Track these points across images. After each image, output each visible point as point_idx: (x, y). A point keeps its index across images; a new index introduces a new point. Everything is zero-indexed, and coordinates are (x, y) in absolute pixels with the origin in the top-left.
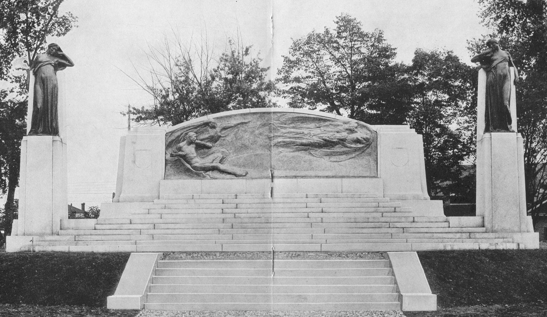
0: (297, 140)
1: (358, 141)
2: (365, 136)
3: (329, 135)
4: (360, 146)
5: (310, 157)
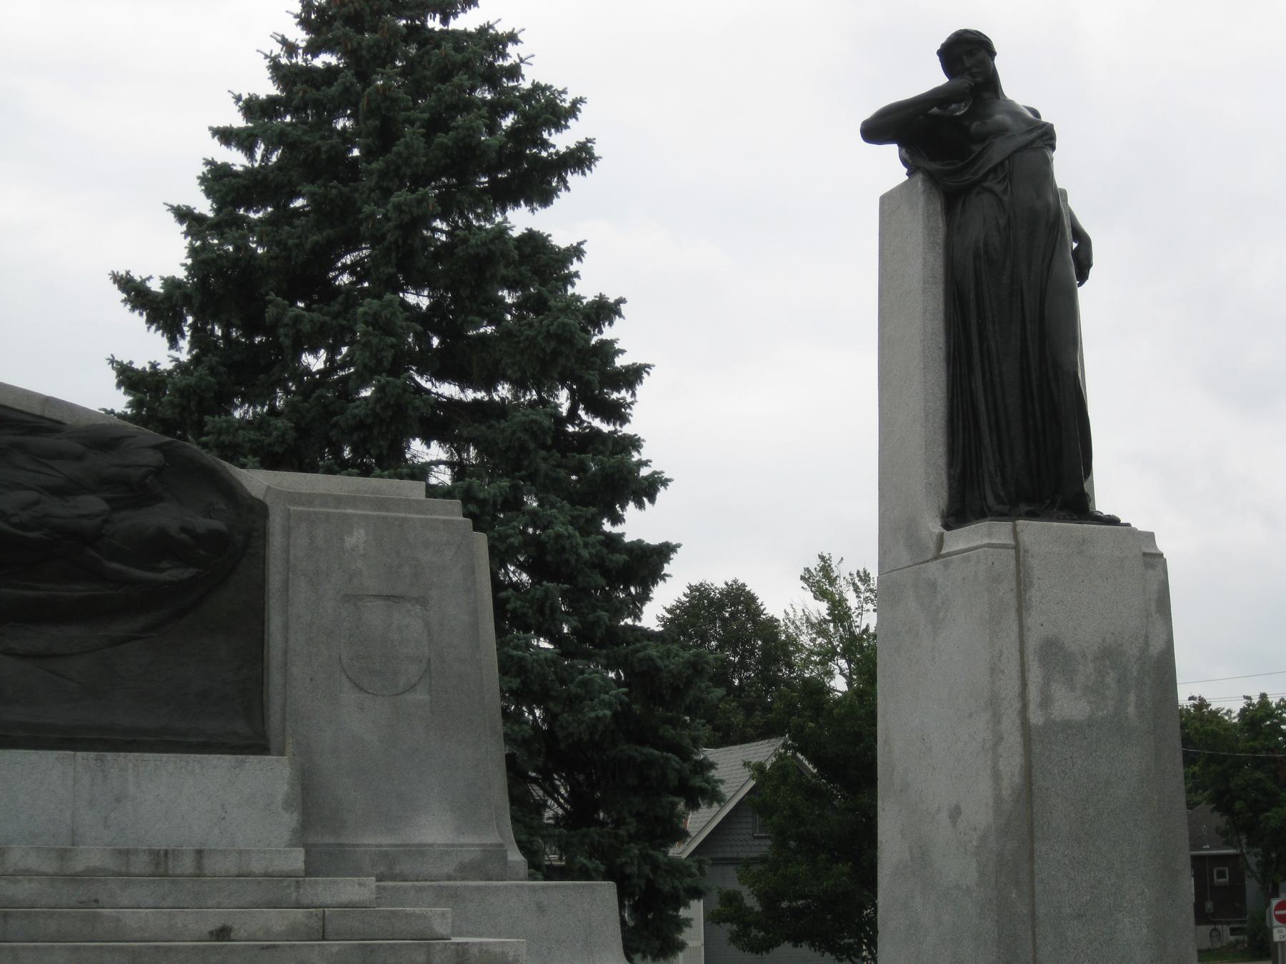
1: (161, 547)
2: (203, 524)
4: (172, 573)
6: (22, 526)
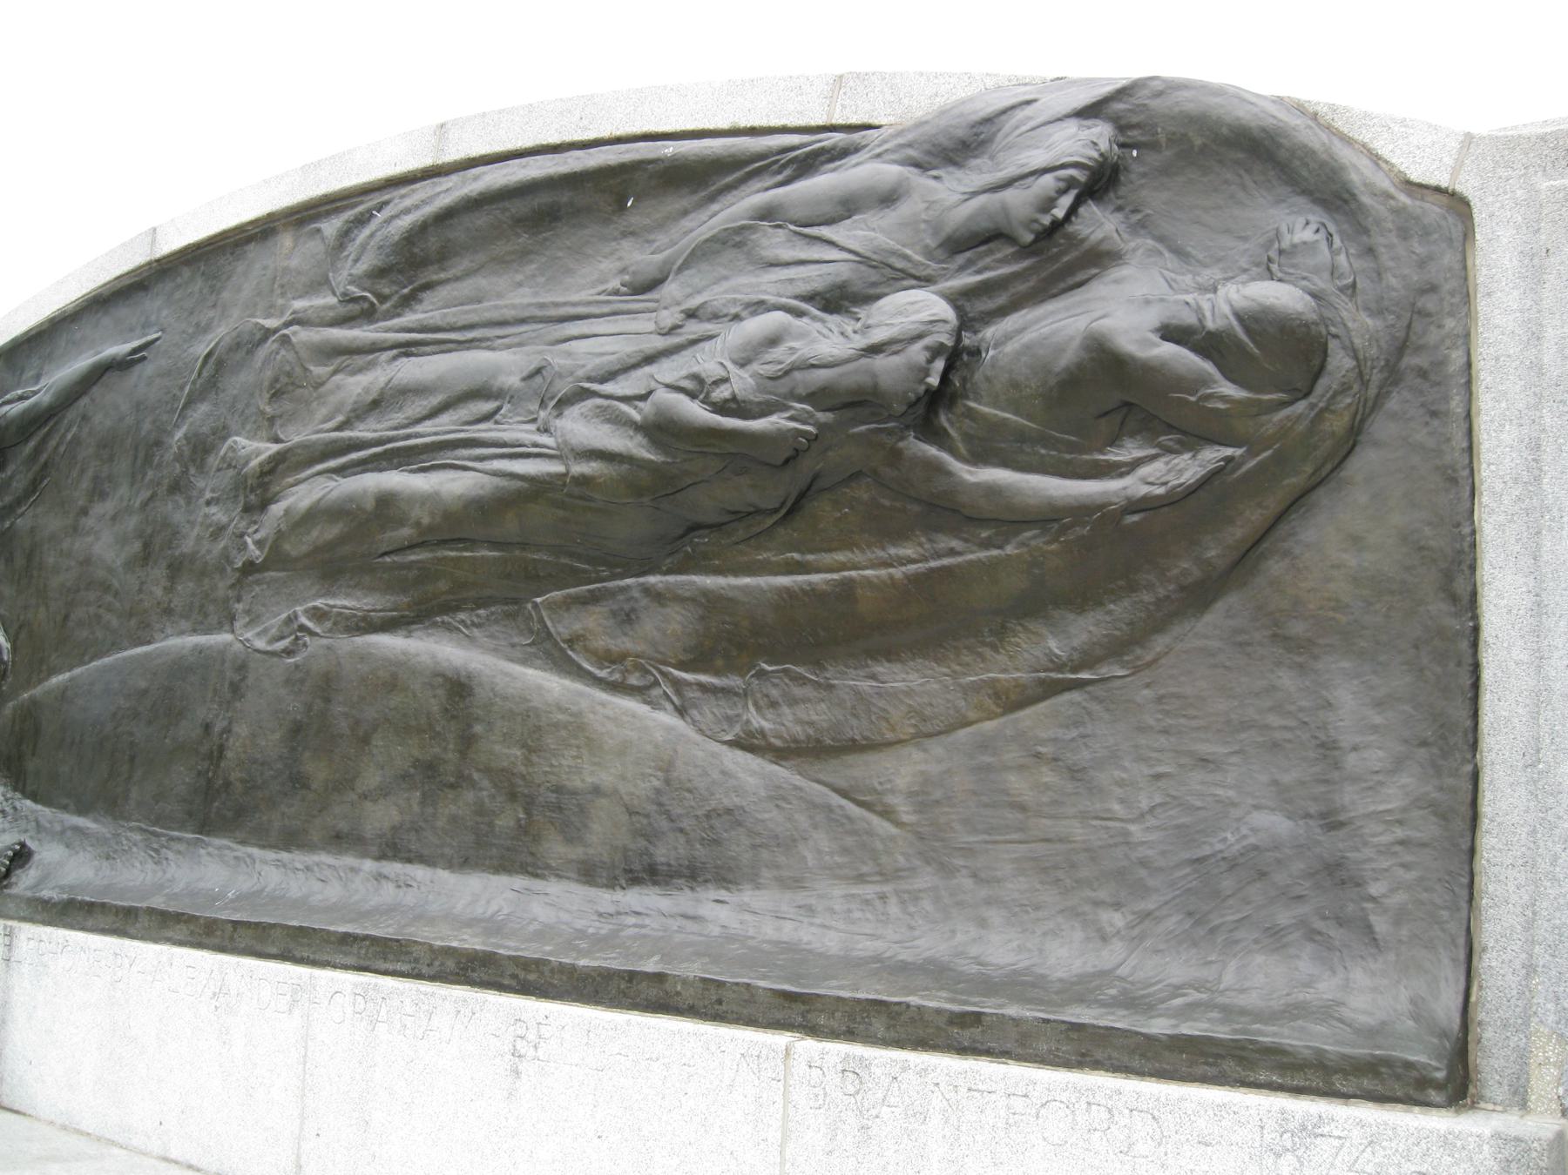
1: (1110, 397)
4: (1154, 472)
5: (547, 685)
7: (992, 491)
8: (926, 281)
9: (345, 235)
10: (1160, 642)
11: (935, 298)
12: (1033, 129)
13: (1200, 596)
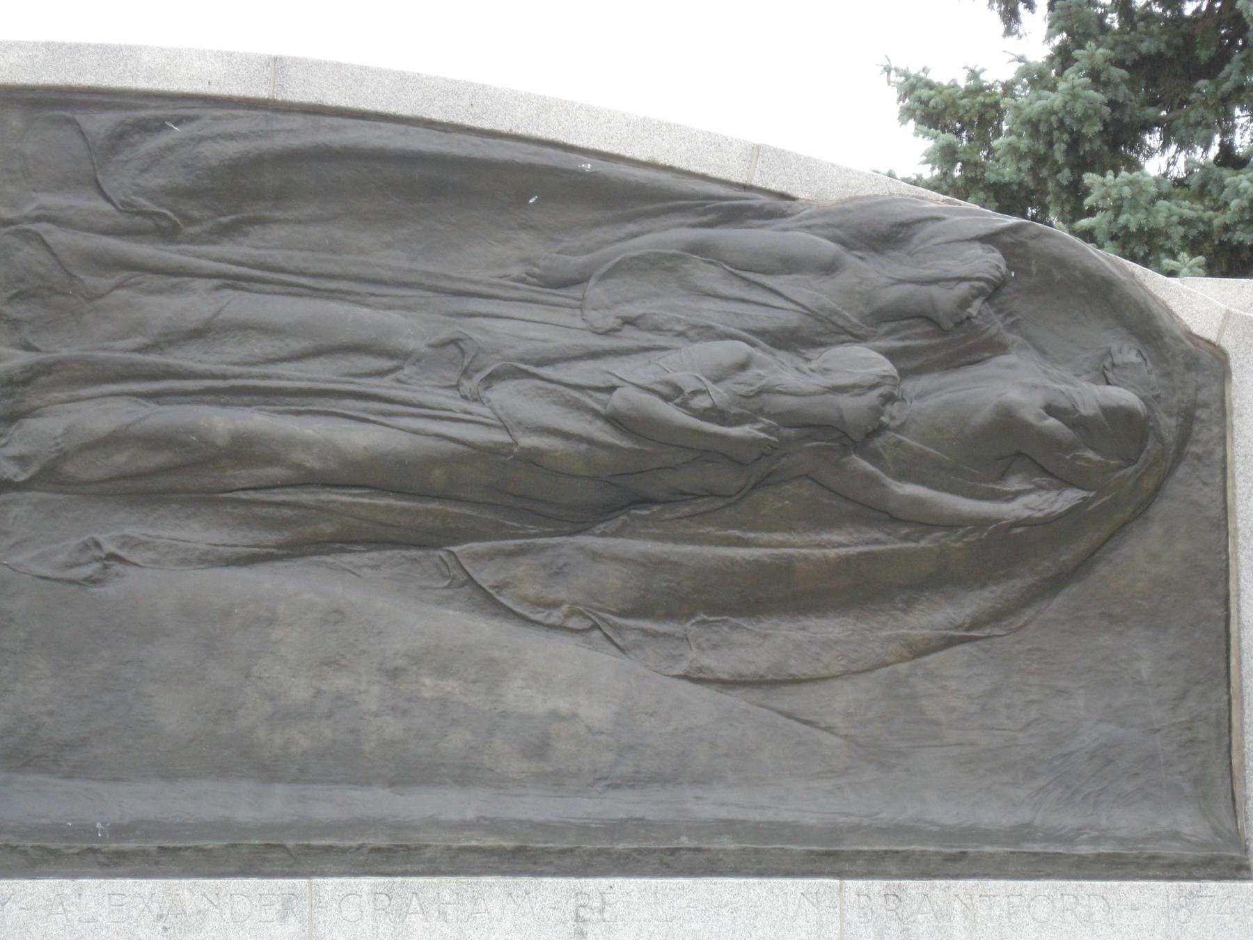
0: (311, 428)
1: (1004, 447)
2: (1093, 396)
3: (687, 363)
4: (1031, 502)
6: (716, 414)
7: (917, 502)
8: (859, 339)
9: (119, 138)
10: (1028, 613)
11: (874, 354)
12: (947, 243)
13: (1055, 584)
